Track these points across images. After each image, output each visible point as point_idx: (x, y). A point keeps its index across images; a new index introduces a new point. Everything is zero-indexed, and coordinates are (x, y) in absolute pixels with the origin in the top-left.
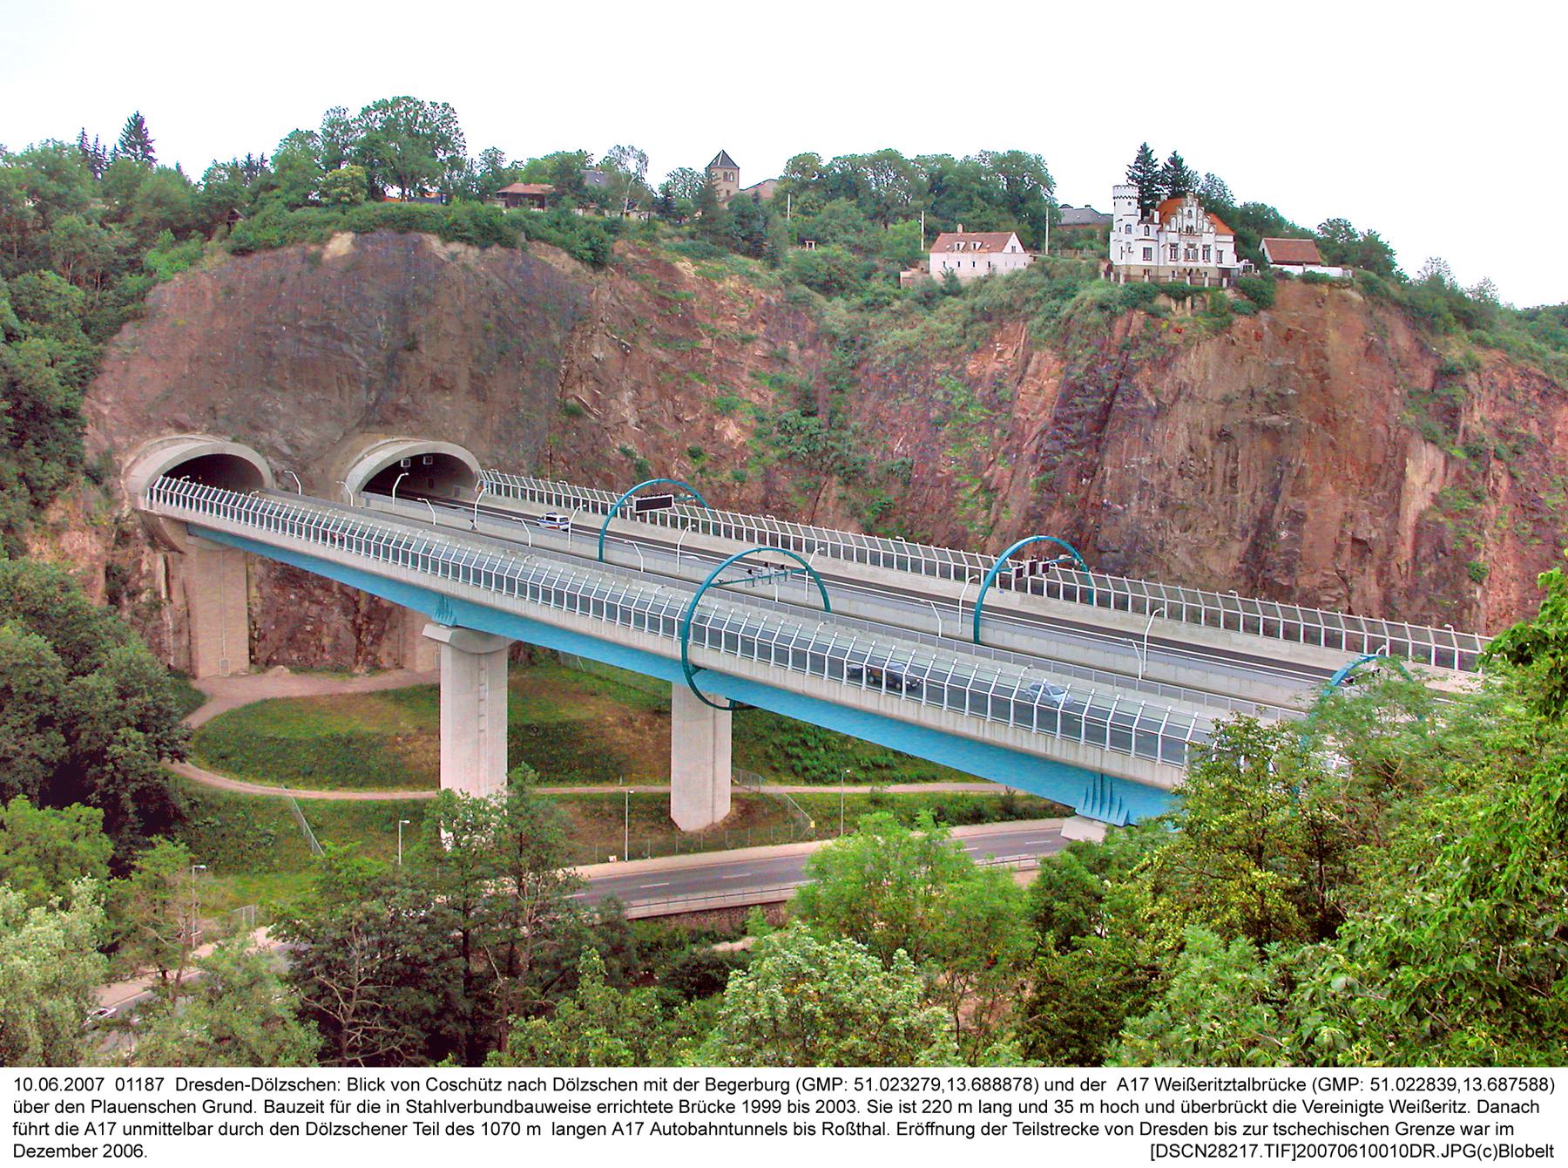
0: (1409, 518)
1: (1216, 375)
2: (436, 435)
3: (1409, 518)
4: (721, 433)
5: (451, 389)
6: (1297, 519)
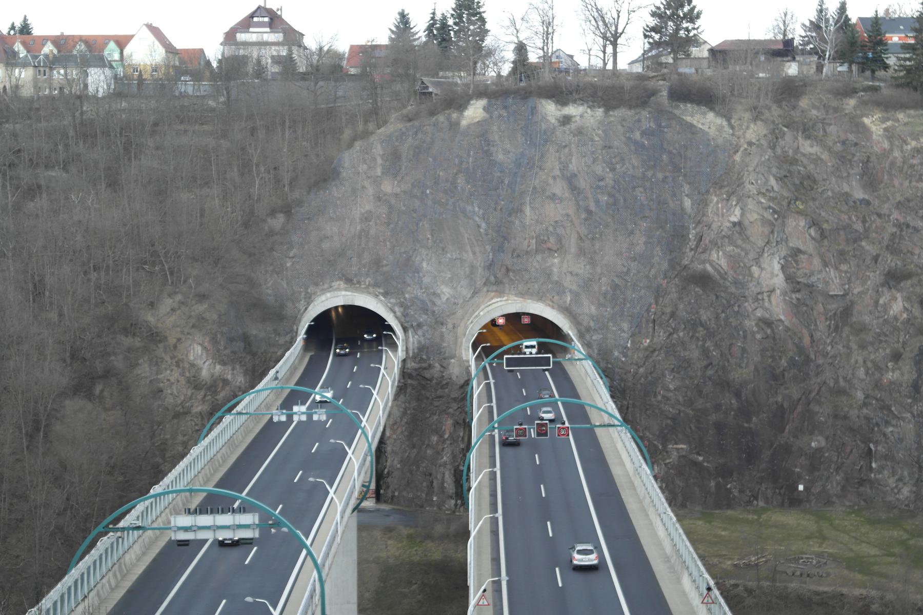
2: (540, 297)
4: (886, 308)
5: (560, 249)
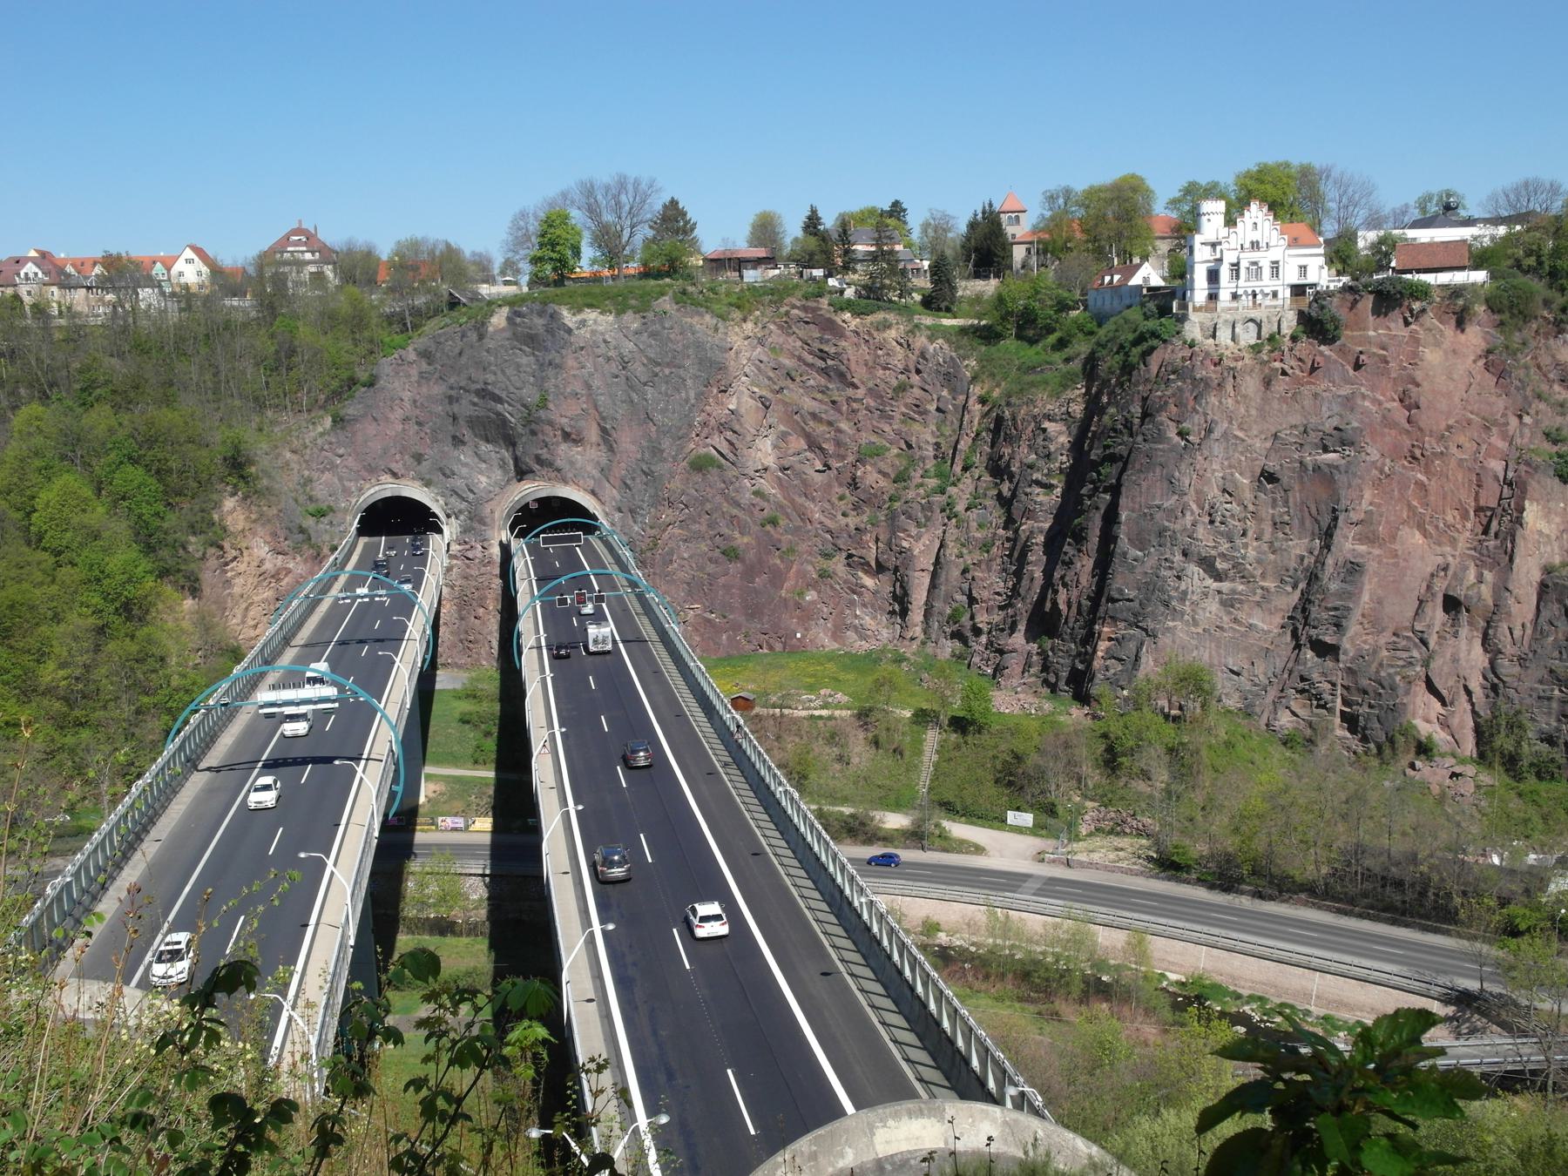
0: (1527, 572)
1: (1261, 410)
3: (1527, 572)
6: (1353, 569)
